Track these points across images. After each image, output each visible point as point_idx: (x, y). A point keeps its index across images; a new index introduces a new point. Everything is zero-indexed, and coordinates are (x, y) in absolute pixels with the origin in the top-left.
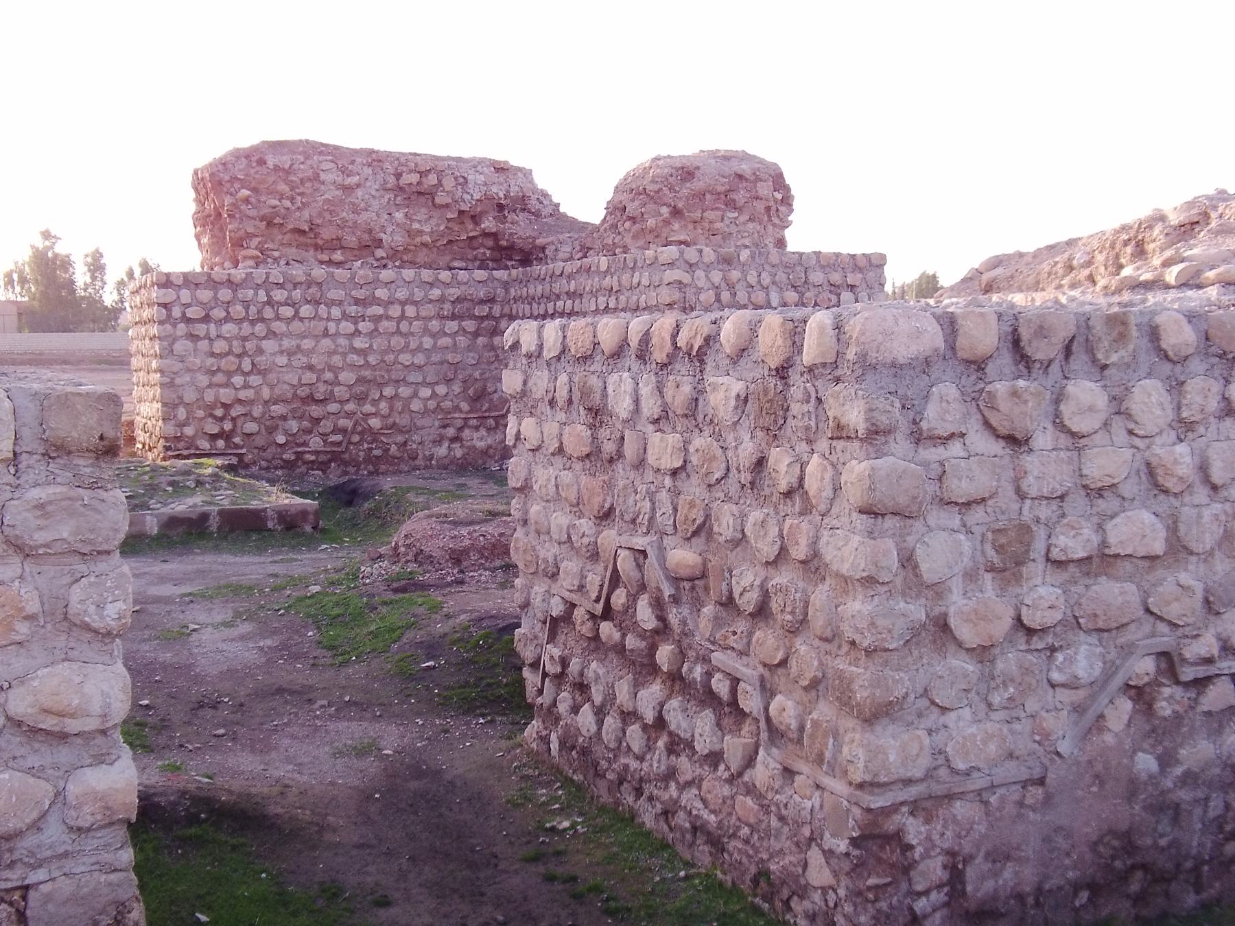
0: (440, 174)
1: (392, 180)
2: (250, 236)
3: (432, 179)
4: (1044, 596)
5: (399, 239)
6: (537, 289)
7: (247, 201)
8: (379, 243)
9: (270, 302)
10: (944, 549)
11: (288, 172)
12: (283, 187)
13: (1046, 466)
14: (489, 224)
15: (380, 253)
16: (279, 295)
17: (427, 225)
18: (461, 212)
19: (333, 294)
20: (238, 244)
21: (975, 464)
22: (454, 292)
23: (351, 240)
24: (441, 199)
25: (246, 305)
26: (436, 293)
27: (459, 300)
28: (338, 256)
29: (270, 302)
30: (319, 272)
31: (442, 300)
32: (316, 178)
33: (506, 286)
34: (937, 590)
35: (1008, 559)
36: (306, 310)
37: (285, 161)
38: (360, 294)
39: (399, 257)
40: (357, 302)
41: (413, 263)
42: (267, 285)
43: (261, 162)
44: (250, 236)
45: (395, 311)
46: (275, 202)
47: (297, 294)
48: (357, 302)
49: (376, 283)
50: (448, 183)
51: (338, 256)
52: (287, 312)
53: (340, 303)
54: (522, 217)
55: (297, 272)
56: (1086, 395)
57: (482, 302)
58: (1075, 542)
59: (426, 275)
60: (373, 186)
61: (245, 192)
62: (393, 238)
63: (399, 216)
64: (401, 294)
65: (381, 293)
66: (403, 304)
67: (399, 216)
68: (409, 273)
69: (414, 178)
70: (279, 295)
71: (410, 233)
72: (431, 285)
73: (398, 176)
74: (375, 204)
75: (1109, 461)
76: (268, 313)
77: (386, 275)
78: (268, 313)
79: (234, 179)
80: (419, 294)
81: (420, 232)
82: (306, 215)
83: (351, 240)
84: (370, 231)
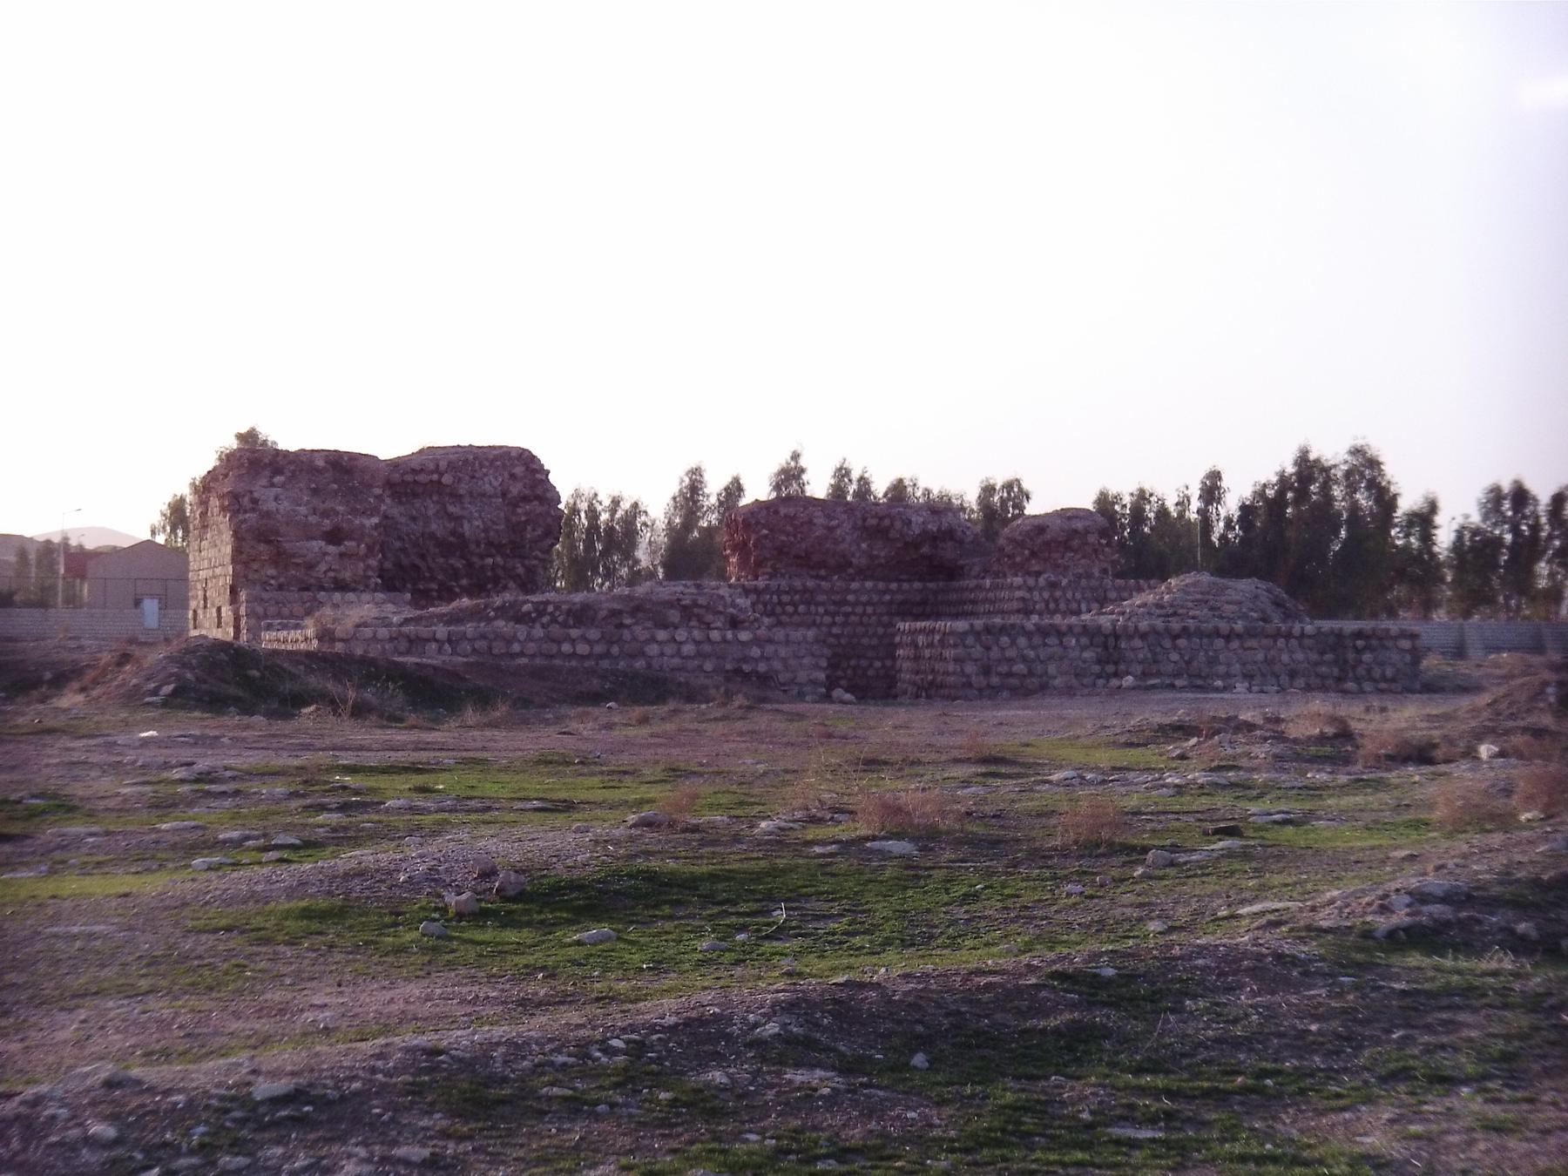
0: (893, 519)
1: (860, 523)
2: (766, 559)
3: (887, 522)
4: (995, 680)
5: (864, 561)
6: (954, 596)
7: (766, 536)
8: (850, 564)
9: (780, 603)
10: (970, 668)
11: (794, 517)
12: (789, 528)
13: (995, 653)
14: (925, 550)
15: (851, 571)
16: (785, 598)
17: (882, 552)
18: (906, 544)
19: (821, 598)
20: (759, 564)
21: (977, 651)
22: (899, 597)
23: (832, 562)
24: (893, 534)
25: (765, 605)
26: (888, 597)
27: (902, 603)
28: (823, 572)
29: (780, 603)
30: (810, 584)
31: (891, 602)
32: (810, 522)
33: (935, 593)
34: (968, 676)
35: (986, 671)
36: (801, 608)
37: (791, 511)
38: (837, 598)
39: (863, 574)
40: (835, 603)
41: (872, 578)
42: (779, 592)
43: (776, 512)
44: (766, 559)
45: (859, 610)
46: (783, 538)
47: (797, 597)
48: (835, 603)
49: (848, 591)
50: (898, 524)
51: (823, 572)
52: (790, 609)
53: (823, 604)
54: (950, 543)
55: (797, 583)
56: (1005, 640)
57: (919, 604)
58: (1004, 669)
59: (881, 585)
60: (847, 526)
61: (765, 532)
62: (859, 561)
63: (864, 546)
64: (864, 598)
65: (850, 598)
66: (865, 605)
67: (864, 546)
68: (869, 584)
69: (874, 522)
70: (785, 598)
71: (872, 557)
72: (885, 592)
73: (864, 520)
74: (848, 538)
75: (1011, 653)
76: (778, 610)
77: (855, 585)
78: (778, 610)
79: (758, 523)
80: (875, 598)
81: (877, 557)
82: (804, 546)
83: (832, 562)
84: (844, 556)
